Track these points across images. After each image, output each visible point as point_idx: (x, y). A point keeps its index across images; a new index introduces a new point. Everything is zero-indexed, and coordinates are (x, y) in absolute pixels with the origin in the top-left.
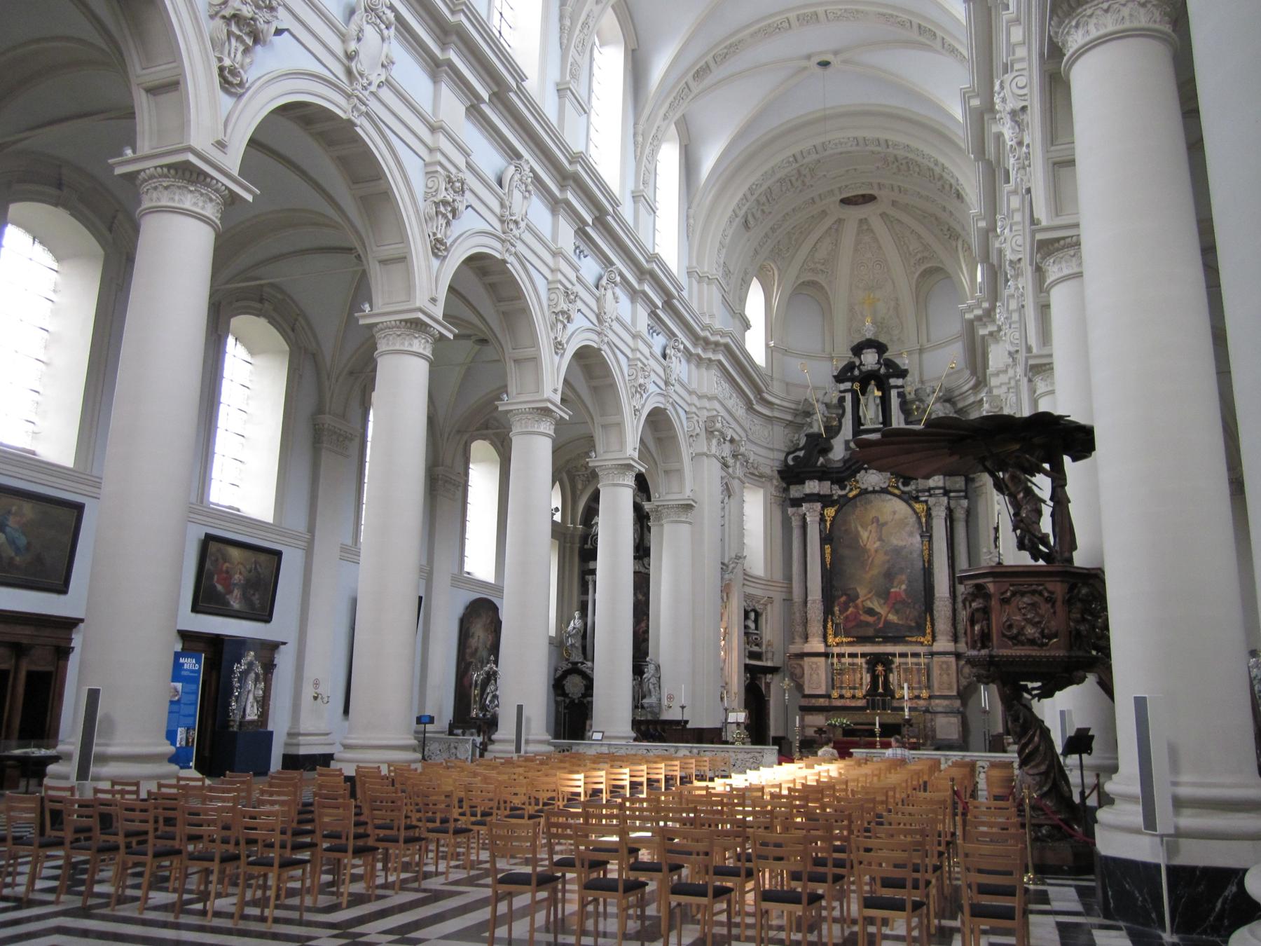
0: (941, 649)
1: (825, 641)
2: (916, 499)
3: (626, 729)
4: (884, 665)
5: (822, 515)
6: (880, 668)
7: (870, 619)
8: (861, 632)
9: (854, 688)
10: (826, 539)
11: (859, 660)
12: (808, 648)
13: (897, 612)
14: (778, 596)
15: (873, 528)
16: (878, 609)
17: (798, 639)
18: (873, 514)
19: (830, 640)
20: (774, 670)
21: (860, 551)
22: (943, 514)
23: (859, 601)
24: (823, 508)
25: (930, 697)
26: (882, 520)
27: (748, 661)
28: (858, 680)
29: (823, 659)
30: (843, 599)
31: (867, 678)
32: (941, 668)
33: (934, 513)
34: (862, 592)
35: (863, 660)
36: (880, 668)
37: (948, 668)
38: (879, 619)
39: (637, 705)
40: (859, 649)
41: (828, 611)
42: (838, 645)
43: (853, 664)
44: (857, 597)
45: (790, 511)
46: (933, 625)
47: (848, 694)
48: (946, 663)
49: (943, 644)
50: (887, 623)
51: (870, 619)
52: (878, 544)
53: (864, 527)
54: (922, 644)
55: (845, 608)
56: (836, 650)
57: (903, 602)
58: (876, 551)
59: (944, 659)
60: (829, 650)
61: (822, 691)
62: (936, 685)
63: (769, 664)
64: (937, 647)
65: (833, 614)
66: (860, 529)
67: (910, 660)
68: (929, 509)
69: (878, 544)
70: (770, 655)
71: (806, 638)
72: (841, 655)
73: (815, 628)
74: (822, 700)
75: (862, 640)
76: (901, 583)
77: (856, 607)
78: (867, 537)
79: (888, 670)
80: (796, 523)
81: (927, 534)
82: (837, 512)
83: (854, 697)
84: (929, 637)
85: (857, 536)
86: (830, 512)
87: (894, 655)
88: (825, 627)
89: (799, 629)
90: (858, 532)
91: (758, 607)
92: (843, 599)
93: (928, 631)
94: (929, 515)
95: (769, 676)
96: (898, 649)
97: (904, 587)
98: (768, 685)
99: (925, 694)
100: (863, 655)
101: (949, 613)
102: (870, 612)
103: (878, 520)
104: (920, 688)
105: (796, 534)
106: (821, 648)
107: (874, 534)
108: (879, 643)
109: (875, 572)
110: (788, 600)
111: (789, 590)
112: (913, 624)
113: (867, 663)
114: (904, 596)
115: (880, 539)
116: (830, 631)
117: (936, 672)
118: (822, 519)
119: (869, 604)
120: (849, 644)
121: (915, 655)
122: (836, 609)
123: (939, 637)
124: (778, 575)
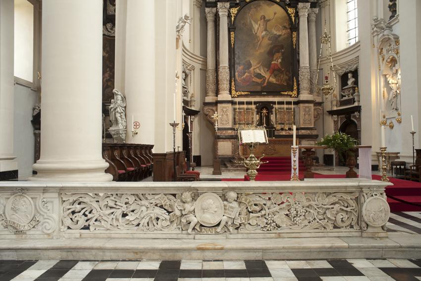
1: (231, 94)
2: (289, 5)
3: (95, 158)
4: (267, 109)
5: (229, 11)
6: (265, 111)
7: (259, 81)
12: (220, 98)
13: (275, 76)
14: (198, 67)
15: (261, 22)
16: (263, 74)
17: (210, 93)
19: (233, 92)
21: (253, 37)
23: (252, 68)
24: (231, 7)
26: (267, 18)
29: (230, 105)
32: (305, 110)
33: (300, 14)
36: (265, 111)
37: (309, 110)
38: (265, 80)
39: (106, 135)
42: (239, 96)
44: (250, 65)
45: (207, 10)
46: (298, 85)
48: (308, 107)
50: (269, 83)
51: (259, 81)
52: (264, 33)
53: (256, 22)
54: (291, 96)
56: (237, 100)
57: (279, 70)
58: (263, 37)
59: (307, 105)
61: (230, 126)
62: (302, 122)
65: (234, 77)
66: (253, 22)
67: (285, 106)
69: (264, 33)
70: (193, 104)
71: (217, 93)
72: (241, 103)
73: (224, 84)
74: (230, 131)
75: (253, 93)
76: (277, 59)
78: (257, 28)
79: (270, 112)
80: (210, 18)
82: (239, 11)
84: (295, 92)
85: (251, 28)
86: (234, 11)
87: (274, 103)
89: (211, 87)
90: (252, 26)
94: (297, 15)
96: (276, 99)
97: (280, 60)
100: (255, 103)
102: (259, 76)
103: (264, 18)
105: (210, 26)
106: (229, 98)
107: (262, 27)
108: (264, 96)
109: (262, 50)
110: (204, 70)
111: (205, 63)
112: (285, 84)
113: (257, 108)
114: (279, 66)
115: (266, 30)
116: (233, 88)
118: (229, 16)
119: (258, 71)
120: (246, 96)
121: (289, 103)
122: (236, 73)
123: (302, 91)
124: (197, 52)
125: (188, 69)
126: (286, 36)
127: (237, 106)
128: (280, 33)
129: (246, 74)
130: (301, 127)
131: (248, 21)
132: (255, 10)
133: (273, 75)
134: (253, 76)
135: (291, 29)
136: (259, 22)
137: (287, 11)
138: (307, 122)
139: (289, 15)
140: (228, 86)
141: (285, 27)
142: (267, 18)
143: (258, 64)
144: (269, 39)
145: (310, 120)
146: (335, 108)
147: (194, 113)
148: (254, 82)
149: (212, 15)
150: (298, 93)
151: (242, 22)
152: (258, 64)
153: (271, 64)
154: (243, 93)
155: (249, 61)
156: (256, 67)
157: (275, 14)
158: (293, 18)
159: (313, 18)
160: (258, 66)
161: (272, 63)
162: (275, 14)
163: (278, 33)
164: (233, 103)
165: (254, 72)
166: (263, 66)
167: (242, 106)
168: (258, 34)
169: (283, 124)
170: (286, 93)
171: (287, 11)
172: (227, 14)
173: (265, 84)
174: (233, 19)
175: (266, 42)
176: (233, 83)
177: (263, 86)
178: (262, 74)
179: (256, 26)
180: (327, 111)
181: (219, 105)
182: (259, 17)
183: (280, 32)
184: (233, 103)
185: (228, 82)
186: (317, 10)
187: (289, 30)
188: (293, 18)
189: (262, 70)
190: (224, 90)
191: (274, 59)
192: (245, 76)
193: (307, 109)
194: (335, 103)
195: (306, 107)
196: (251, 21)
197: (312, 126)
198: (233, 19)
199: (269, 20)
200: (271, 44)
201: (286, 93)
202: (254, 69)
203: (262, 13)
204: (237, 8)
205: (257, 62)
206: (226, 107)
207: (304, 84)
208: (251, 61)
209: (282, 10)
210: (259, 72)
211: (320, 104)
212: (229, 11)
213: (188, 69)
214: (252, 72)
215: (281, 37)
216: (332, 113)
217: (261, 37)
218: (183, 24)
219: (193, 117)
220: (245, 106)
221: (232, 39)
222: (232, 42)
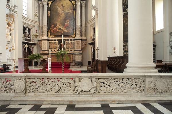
0: (77, 38)
5: (48, 3)
7: (60, 31)
8: (57, 35)
9: (55, 49)
10: (49, 9)
11: (57, 41)
12: (43, 38)
13: (67, 29)
14: (36, 25)
16: (62, 28)
18: (61, 4)
19: (49, 36)
20: (34, 44)
21: (57, 13)
22: (79, 4)
23: (57, 26)
25: (74, 51)
26: (63, 6)
27: (24, 41)
28: (56, 47)
29: (47, 41)
30: (53, 26)
31: (58, 46)
32: (77, 43)
33: (77, 3)
34: (58, 24)
35: (58, 41)
38: (62, 31)
40: (57, 39)
41: (49, 29)
42: (51, 37)
43: (55, 42)
47: (53, 50)
48: (79, 42)
49: (78, 37)
51: (60, 31)
52: (62, 11)
53: (59, 7)
54: (73, 37)
55: (53, 28)
58: (62, 13)
59: (78, 41)
60: (49, 39)
61: (46, 49)
63: (33, 43)
64: (77, 38)
66: (58, 7)
68: (76, 3)
69: (62, 11)
71: (43, 36)
73: (45, 33)
77: (56, 28)
78: (60, 9)
80: (41, 6)
81: (75, 9)
82: (52, 3)
83: (55, 51)
85: (57, 10)
88: (48, 33)
91: (30, 28)
92: (53, 26)
93: (75, 34)
94: (76, 4)
95: (33, 46)
98: (33, 48)
99: (73, 50)
100: (58, 40)
101: (80, 29)
102: (60, 29)
104: (72, 48)
106: (46, 38)
107: (61, 9)
109: (61, 19)
115: (63, 10)
116: (49, 34)
117: (76, 44)
118: (48, 5)
119: (59, 27)
120: (54, 37)
122: (51, 28)
125: (31, 27)
126: (71, 13)
127: (50, 41)
128: (69, 12)
129: (55, 28)
130: (76, 50)
131: (56, 7)
132: (59, 2)
133: (66, 29)
135: (73, 10)
136: (60, 7)
137: (72, 2)
138: (78, 47)
139: (72, 4)
140: (47, 33)
141: (71, 9)
142: (63, 6)
143: (60, 24)
144: (64, 14)
145: (79, 47)
146: (91, 42)
147: (90, 44)
149: (41, 4)
150: (76, 36)
151: (53, 7)
152: (60, 24)
153: (65, 24)
154: (53, 36)
157: (67, 3)
158: (74, 5)
159: (83, 5)
161: (66, 23)
162: (67, 3)
163: (68, 12)
164: (48, 40)
167: (52, 41)
168: (60, 12)
169: (69, 48)
170: (71, 36)
171: (72, 2)
172: (46, 4)
174: (49, 6)
175: (63, 15)
176: (49, 32)
179: (59, 9)
180: (89, 43)
181: (42, 41)
182: (60, 6)
183: (69, 11)
184: (48, 40)
185: (47, 32)
186: (85, 2)
187: (73, 10)
188: (74, 5)
189: (61, 27)
190: (44, 35)
191: (66, 22)
192: (54, 29)
193: (78, 42)
194: (91, 40)
195: (78, 42)
196: (57, 7)
197: (80, 49)
198: (49, 6)
199: (64, 6)
200: (65, 16)
201: (71, 36)
203: (61, 4)
204: (51, 2)
205: (59, 23)
206: (45, 42)
207: (78, 32)
209: (70, 2)
211: (86, 40)
212: (48, 3)
213: (31, 27)
214: (57, 27)
215: (69, 13)
216: (90, 44)
217: (61, 13)
218: (14, 8)
219: (33, 46)
220: (53, 41)
221: (49, 14)
222: (49, 15)
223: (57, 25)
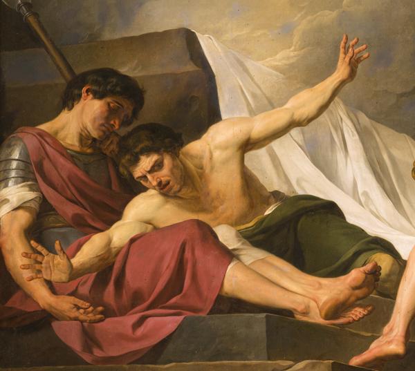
7: (307, 293)
23: (213, 146)
30: (79, 120)
38: (380, 290)
44: (198, 107)
51: (307, 293)
77: (187, 186)
92: (79, 120)
102: (306, 231)
119: (294, 171)
129: (144, 209)
134: (226, 235)
148: (236, 305)
152: (311, 74)
155: (190, 39)
156: (278, 118)
160: (305, 101)
165: (249, 182)
166: (355, 107)
173: (391, 341)
177: (355, 361)
178: (354, 215)
189: (353, 166)
192: (120, 233)
202: (248, 145)
205: (287, 55)
208: (208, 45)
210: (323, 189)
214: (224, 180)
223: (214, 116)
